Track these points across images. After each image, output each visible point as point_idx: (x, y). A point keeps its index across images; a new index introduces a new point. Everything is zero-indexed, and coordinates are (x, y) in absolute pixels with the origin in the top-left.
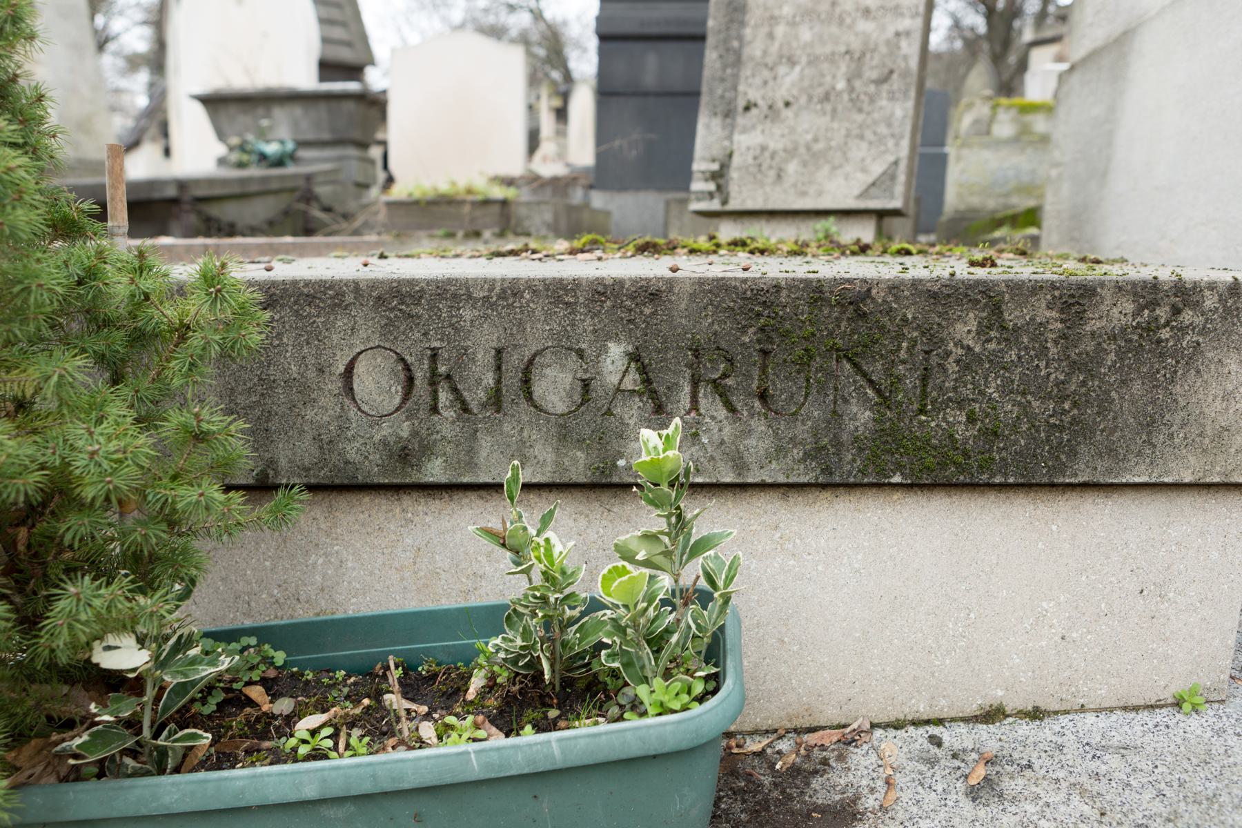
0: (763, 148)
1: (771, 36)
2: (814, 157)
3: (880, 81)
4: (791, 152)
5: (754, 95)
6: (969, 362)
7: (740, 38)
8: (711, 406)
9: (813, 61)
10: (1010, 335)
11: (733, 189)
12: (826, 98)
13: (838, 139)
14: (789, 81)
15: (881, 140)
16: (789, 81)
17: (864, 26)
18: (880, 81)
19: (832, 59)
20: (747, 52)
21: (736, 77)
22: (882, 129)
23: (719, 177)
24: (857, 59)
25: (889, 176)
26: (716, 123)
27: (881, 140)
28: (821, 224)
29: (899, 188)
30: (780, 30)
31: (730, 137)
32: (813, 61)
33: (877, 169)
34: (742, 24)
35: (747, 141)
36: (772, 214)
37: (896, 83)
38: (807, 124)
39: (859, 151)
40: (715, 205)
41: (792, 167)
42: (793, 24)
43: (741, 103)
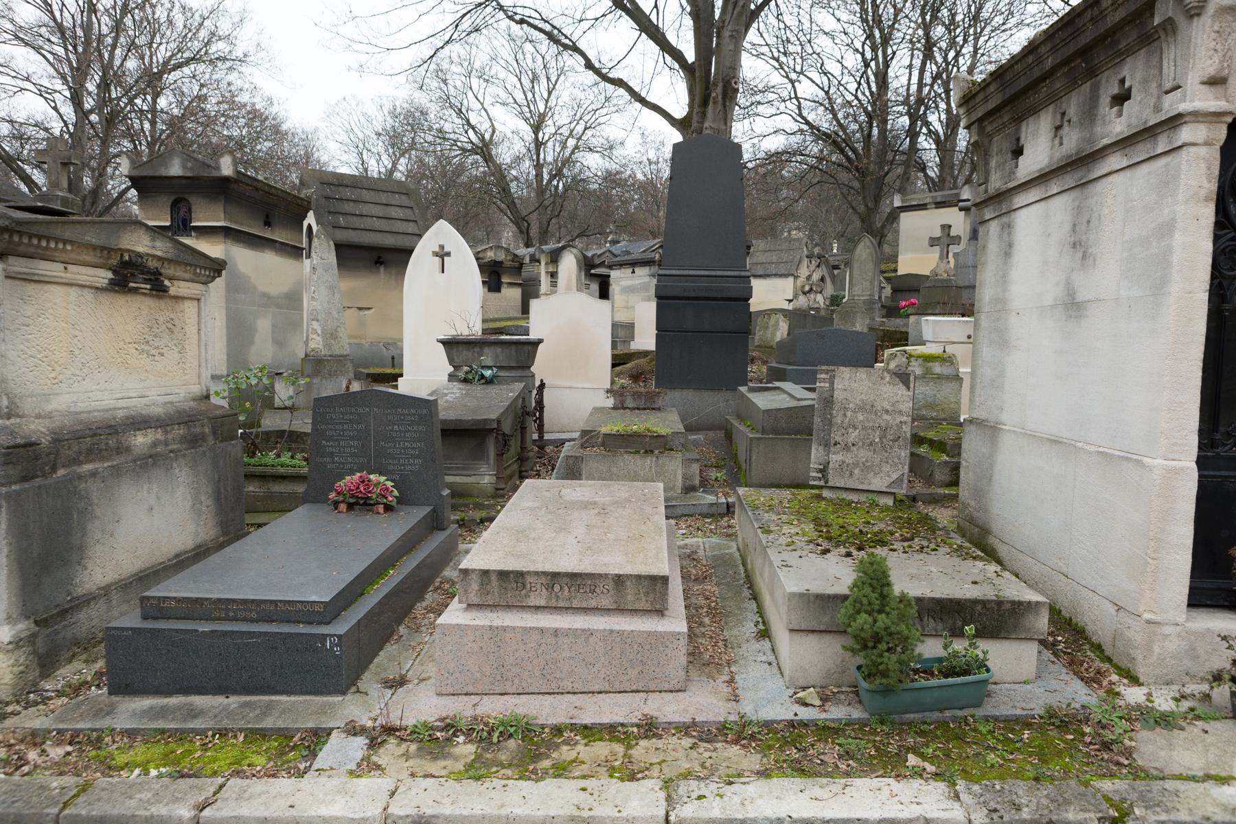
0: (843, 462)
1: (845, 415)
2: (866, 468)
3: (895, 441)
4: (856, 465)
5: (838, 439)
6: (980, 614)
7: (831, 414)
8: (931, 620)
9: (864, 428)
10: (988, 609)
11: (830, 477)
12: (871, 444)
13: (877, 461)
14: (854, 435)
15: (896, 465)
16: (854, 435)
17: (885, 417)
18: (895, 441)
19: (873, 428)
20: (834, 420)
21: (830, 430)
22: (896, 460)
23: (823, 471)
24: (884, 430)
25: (899, 480)
26: (821, 448)
27: (896, 465)
28: (871, 496)
29: (905, 486)
30: (849, 414)
31: (828, 455)
32: (864, 428)
33: (895, 476)
34: (832, 408)
35: (835, 458)
36: (846, 489)
37: (901, 441)
38: (863, 454)
39: (886, 468)
40: (822, 483)
41: (857, 471)
42: (854, 411)
43: (833, 442)
